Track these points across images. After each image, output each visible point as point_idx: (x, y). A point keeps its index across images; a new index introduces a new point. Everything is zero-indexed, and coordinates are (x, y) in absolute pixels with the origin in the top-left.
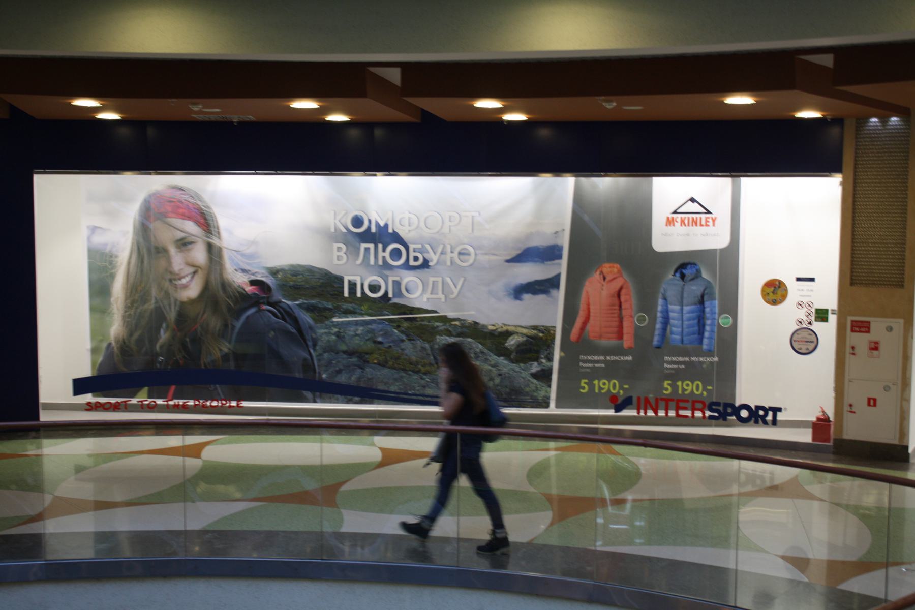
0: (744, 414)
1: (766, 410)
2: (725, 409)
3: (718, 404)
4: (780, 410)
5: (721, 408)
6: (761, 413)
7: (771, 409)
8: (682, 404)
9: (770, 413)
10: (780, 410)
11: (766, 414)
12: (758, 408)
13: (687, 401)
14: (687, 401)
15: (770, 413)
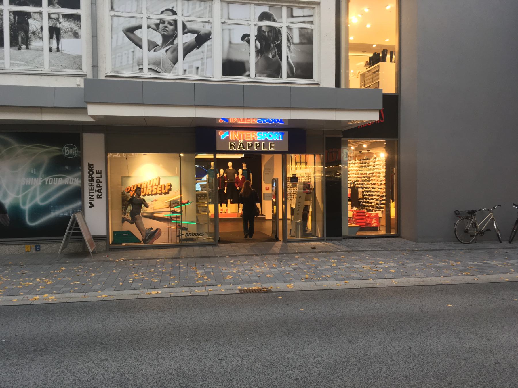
0: (91, 173)
1: (89, 167)
2: (90, 178)
3: (89, 179)
4: (89, 164)
5: (90, 179)
6: (90, 168)
7: (89, 166)
8: (90, 189)
9: (90, 166)
10: (89, 164)
11: (91, 167)
12: (89, 169)
13: (89, 188)
14: (89, 188)
15: (90, 166)
